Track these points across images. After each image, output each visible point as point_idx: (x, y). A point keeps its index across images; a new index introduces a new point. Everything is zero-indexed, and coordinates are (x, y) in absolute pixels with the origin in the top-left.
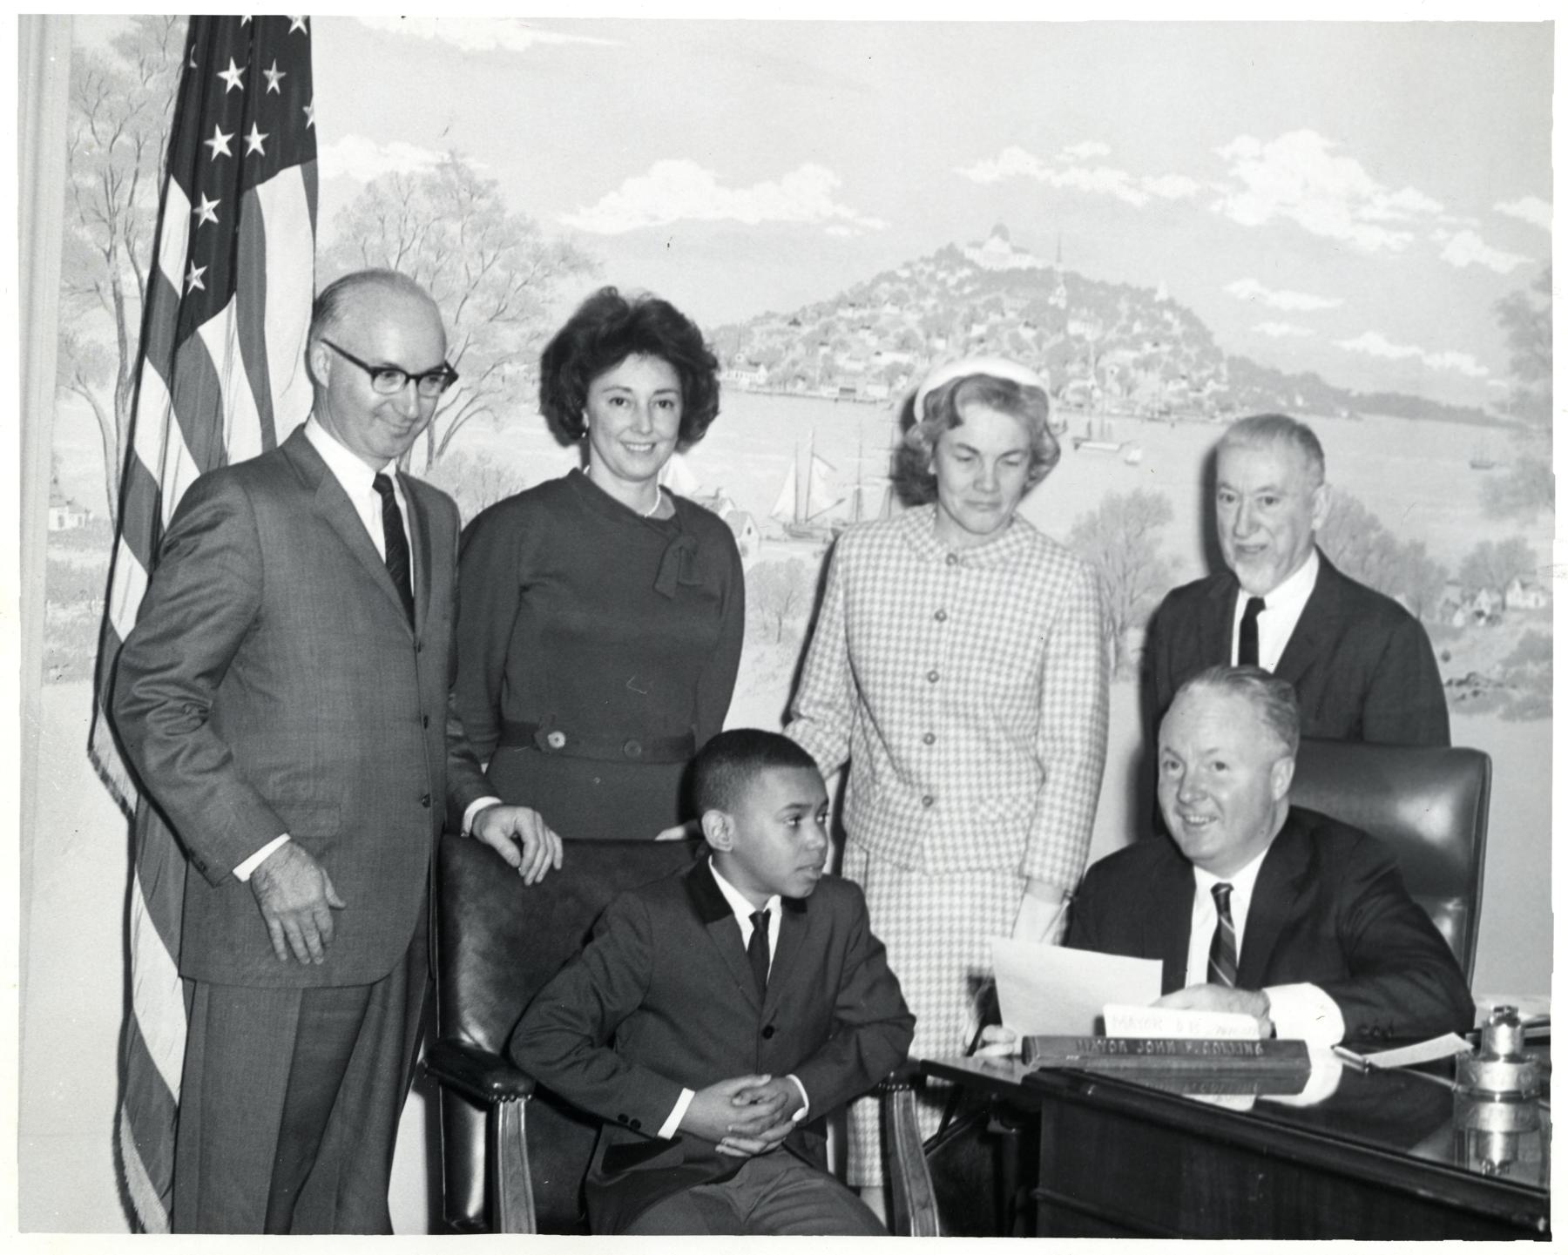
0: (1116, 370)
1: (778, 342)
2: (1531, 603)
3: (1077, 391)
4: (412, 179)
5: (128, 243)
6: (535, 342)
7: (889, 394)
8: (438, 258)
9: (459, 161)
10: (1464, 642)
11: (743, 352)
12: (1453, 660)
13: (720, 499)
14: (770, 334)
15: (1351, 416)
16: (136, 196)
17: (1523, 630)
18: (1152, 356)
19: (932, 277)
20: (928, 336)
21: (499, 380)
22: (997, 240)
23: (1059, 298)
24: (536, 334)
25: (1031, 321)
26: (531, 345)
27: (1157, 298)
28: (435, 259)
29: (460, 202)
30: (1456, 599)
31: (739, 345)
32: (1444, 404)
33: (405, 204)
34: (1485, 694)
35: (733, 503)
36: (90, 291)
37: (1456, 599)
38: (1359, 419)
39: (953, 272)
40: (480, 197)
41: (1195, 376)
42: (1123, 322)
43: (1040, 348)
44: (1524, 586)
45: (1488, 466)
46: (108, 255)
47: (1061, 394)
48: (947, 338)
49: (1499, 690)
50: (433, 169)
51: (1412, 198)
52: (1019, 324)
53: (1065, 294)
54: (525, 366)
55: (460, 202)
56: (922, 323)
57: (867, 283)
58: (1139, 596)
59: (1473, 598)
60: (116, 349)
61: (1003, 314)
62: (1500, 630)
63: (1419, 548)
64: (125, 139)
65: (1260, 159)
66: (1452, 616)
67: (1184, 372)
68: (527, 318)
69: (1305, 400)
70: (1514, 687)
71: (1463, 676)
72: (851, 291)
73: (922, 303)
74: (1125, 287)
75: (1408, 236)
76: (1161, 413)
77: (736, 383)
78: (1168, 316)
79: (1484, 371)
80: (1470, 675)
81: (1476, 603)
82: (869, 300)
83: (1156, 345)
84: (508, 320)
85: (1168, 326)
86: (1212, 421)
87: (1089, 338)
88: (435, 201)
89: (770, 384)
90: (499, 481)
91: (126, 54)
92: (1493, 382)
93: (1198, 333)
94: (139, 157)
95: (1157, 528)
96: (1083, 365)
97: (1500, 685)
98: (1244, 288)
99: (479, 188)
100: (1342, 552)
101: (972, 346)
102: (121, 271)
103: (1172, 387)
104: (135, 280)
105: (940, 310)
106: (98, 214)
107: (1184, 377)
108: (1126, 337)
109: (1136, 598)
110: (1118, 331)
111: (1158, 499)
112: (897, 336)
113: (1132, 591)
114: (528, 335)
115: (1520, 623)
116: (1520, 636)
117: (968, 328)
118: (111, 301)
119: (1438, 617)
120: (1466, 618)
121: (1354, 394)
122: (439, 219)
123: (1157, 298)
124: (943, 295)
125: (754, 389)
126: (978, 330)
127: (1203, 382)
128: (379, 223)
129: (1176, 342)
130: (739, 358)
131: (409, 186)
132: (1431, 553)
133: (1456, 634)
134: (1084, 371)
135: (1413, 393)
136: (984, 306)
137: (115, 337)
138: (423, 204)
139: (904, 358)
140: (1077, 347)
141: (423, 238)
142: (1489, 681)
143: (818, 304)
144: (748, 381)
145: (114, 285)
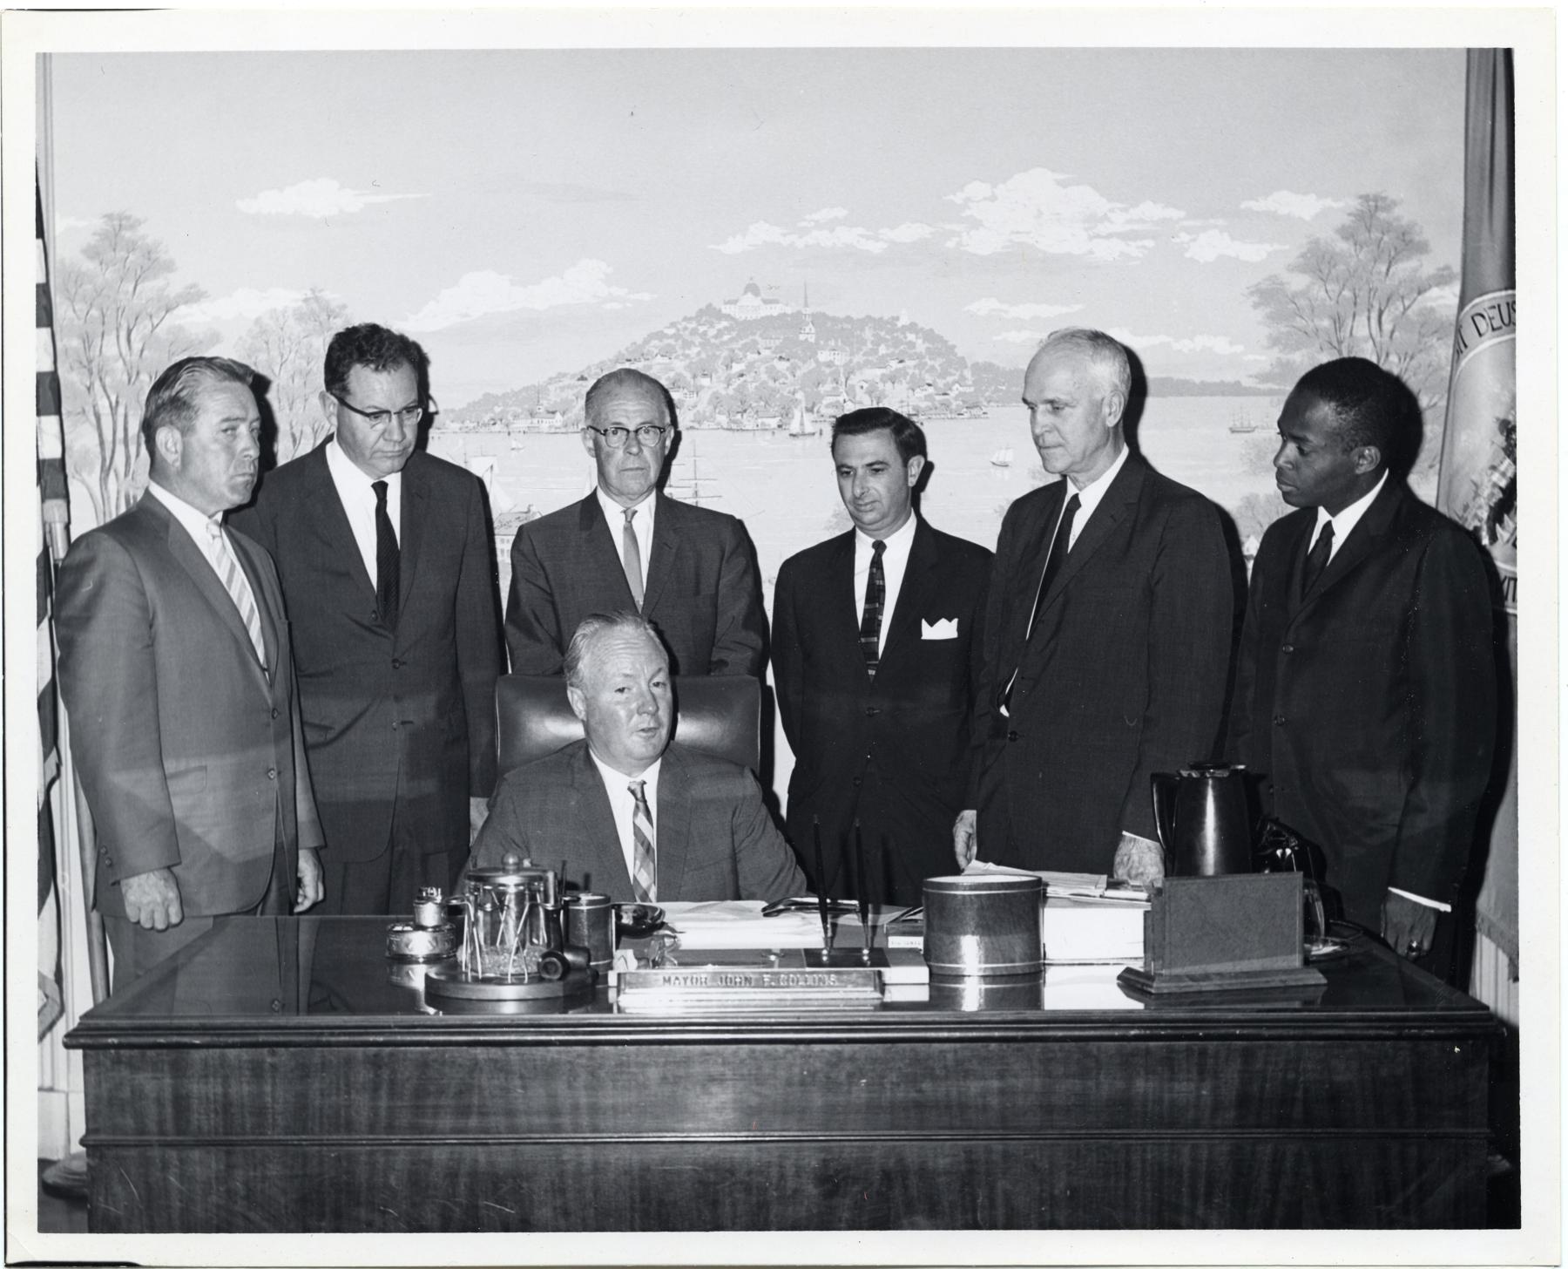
0: (865, 385)
1: (570, 394)
3: (827, 406)
4: (286, 312)
5: (101, 379)
8: (308, 363)
9: (319, 295)
14: (562, 389)
16: (104, 349)
18: (897, 370)
19: (694, 332)
20: (695, 377)
22: (749, 295)
23: (809, 334)
25: (784, 355)
27: (899, 324)
28: (305, 364)
29: (321, 323)
32: (1197, 380)
33: (282, 329)
36: (79, 413)
39: (712, 326)
40: (335, 318)
41: (941, 383)
42: (870, 346)
46: (89, 389)
47: (815, 410)
50: (300, 303)
51: (1151, 210)
52: (773, 359)
53: (813, 331)
55: (321, 323)
56: (688, 367)
57: (640, 342)
60: (98, 449)
61: (759, 353)
64: (95, 313)
65: (993, 198)
67: (931, 382)
72: (627, 349)
73: (687, 352)
74: (869, 317)
75: (1150, 243)
78: (911, 337)
79: (1239, 348)
82: (643, 355)
83: (901, 362)
85: (912, 345)
87: (837, 363)
88: (303, 325)
89: (566, 426)
91: (91, 258)
92: (1251, 357)
93: (939, 346)
94: (103, 323)
96: (835, 385)
98: (983, 306)
99: (333, 311)
102: (98, 398)
103: (919, 393)
104: (107, 403)
105: (703, 356)
106: (81, 363)
107: (929, 385)
108: (870, 358)
110: (864, 355)
117: (728, 367)
118: (93, 419)
122: (306, 337)
123: (899, 324)
124: (705, 344)
125: (553, 430)
126: (737, 368)
128: (265, 345)
129: (920, 356)
131: (284, 316)
134: (834, 388)
136: (739, 349)
137: (96, 441)
138: (294, 328)
140: (828, 371)
141: (297, 351)
143: (602, 362)
144: (547, 425)
145: (94, 407)
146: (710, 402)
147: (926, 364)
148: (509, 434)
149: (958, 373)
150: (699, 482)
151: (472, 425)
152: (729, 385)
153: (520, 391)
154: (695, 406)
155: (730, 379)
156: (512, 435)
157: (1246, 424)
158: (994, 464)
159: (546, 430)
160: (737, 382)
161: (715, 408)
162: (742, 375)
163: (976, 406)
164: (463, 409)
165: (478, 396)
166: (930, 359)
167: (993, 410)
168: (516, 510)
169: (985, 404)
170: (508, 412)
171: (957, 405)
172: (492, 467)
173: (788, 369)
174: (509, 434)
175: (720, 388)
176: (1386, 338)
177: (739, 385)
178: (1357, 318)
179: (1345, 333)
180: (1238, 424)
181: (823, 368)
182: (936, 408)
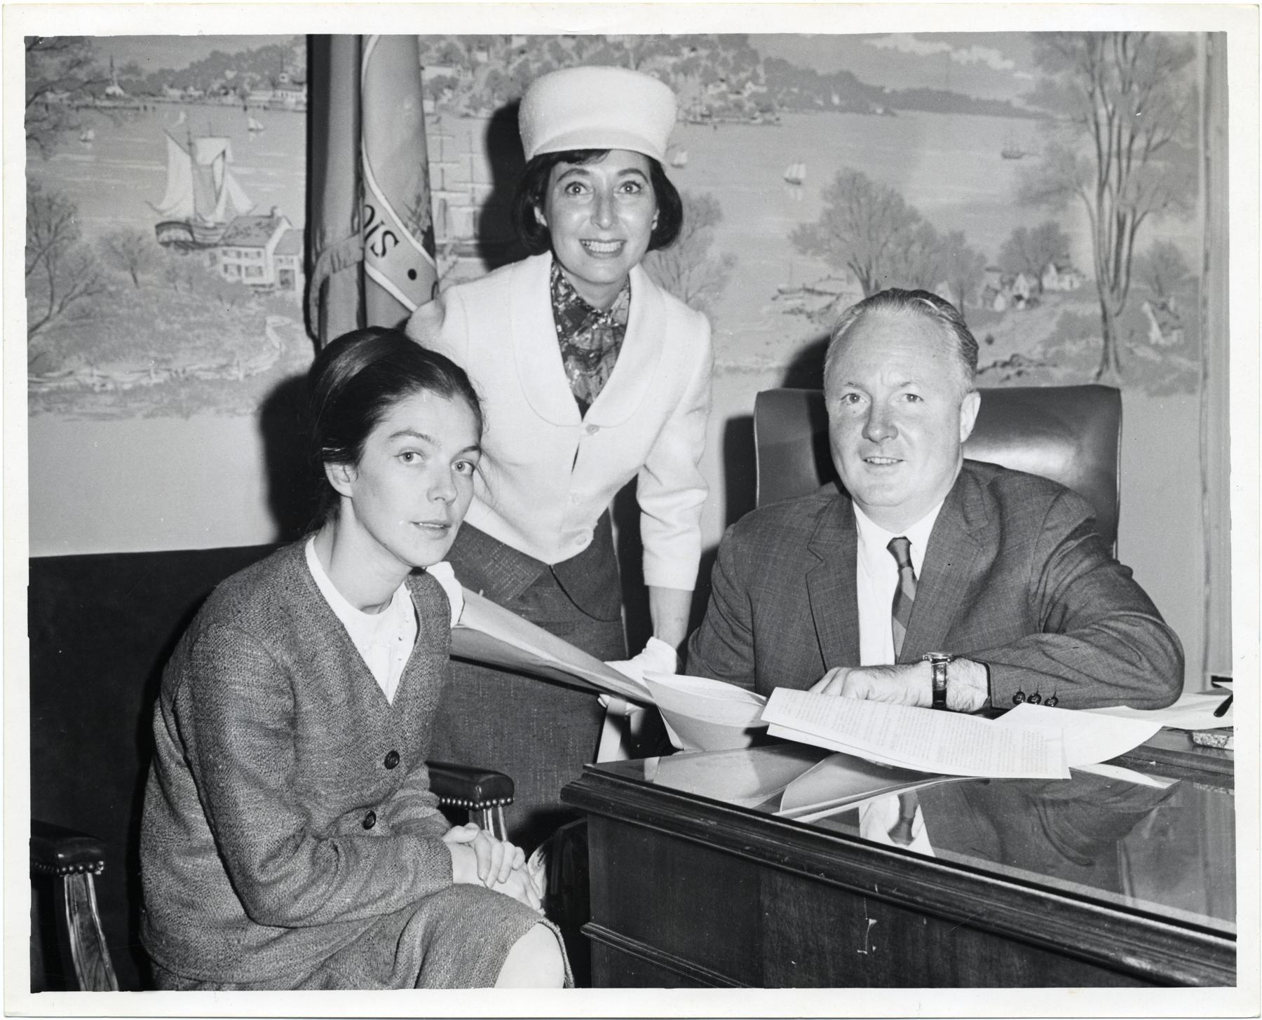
2: (1066, 285)
6: (75, 70)
7: (435, 108)
10: (1006, 325)
11: (286, 72)
12: (997, 342)
13: (275, 218)
15: (886, 112)
17: (1059, 311)
18: (690, 60)
20: (469, 50)
21: (43, 109)
24: (75, 63)
26: (71, 72)
30: (997, 286)
31: (282, 67)
34: (1028, 374)
35: (290, 223)
37: (997, 286)
38: (893, 115)
41: (734, 80)
43: (580, 57)
44: (1059, 270)
45: (1019, 156)
48: (488, 51)
49: (1040, 368)
54: (67, 94)
58: (694, 295)
59: (1012, 282)
62: (1038, 312)
63: (959, 237)
66: (992, 301)
67: (722, 76)
68: (66, 46)
69: (841, 99)
70: (1055, 366)
71: (1007, 358)
76: (703, 116)
77: (282, 103)
79: (1009, 64)
80: (1014, 356)
81: (1014, 289)
83: (693, 49)
84: (46, 49)
86: (754, 122)
90: (50, 208)
92: (1019, 75)
95: (707, 227)
97: (1042, 365)
100: (885, 244)
101: (513, 57)
103: (712, 90)
107: (722, 81)
109: (690, 299)
111: (706, 202)
112: (438, 50)
113: (687, 290)
114: (68, 63)
115: (1056, 305)
116: (1056, 319)
119: (980, 302)
120: (1007, 302)
121: (887, 91)
127: (742, 85)
130: (283, 78)
132: (971, 241)
133: (998, 317)
135: (942, 88)
139: (448, 72)
142: (1031, 361)
144: (294, 100)
146: (487, 84)
147: (718, 54)
148: (245, 108)
149: (751, 69)
150: (477, 186)
151: (196, 94)
152: (509, 63)
153: (260, 52)
154: (470, 88)
155: (510, 55)
156: (250, 111)
157: (1015, 149)
158: (787, 180)
159: (292, 107)
160: (518, 60)
161: (494, 91)
162: (522, 52)
163: (766, 109)
164: (185, 71)
165: (203, 54)
166: (725, 49)
167: (786, 116)
168: (256, 213)
169: (778, 107)
170: (243, 79)
171: (751, 109)
172: (224, 153)
173: (574, 48)
174: (245, 108)
175: (499, 65)
176: (1129, 66)
177: (520, 65)
178: (1107, 41)
179: (1097, 57)
180: (1009, 149)
181: (612, 51)
182: (729, 109)
